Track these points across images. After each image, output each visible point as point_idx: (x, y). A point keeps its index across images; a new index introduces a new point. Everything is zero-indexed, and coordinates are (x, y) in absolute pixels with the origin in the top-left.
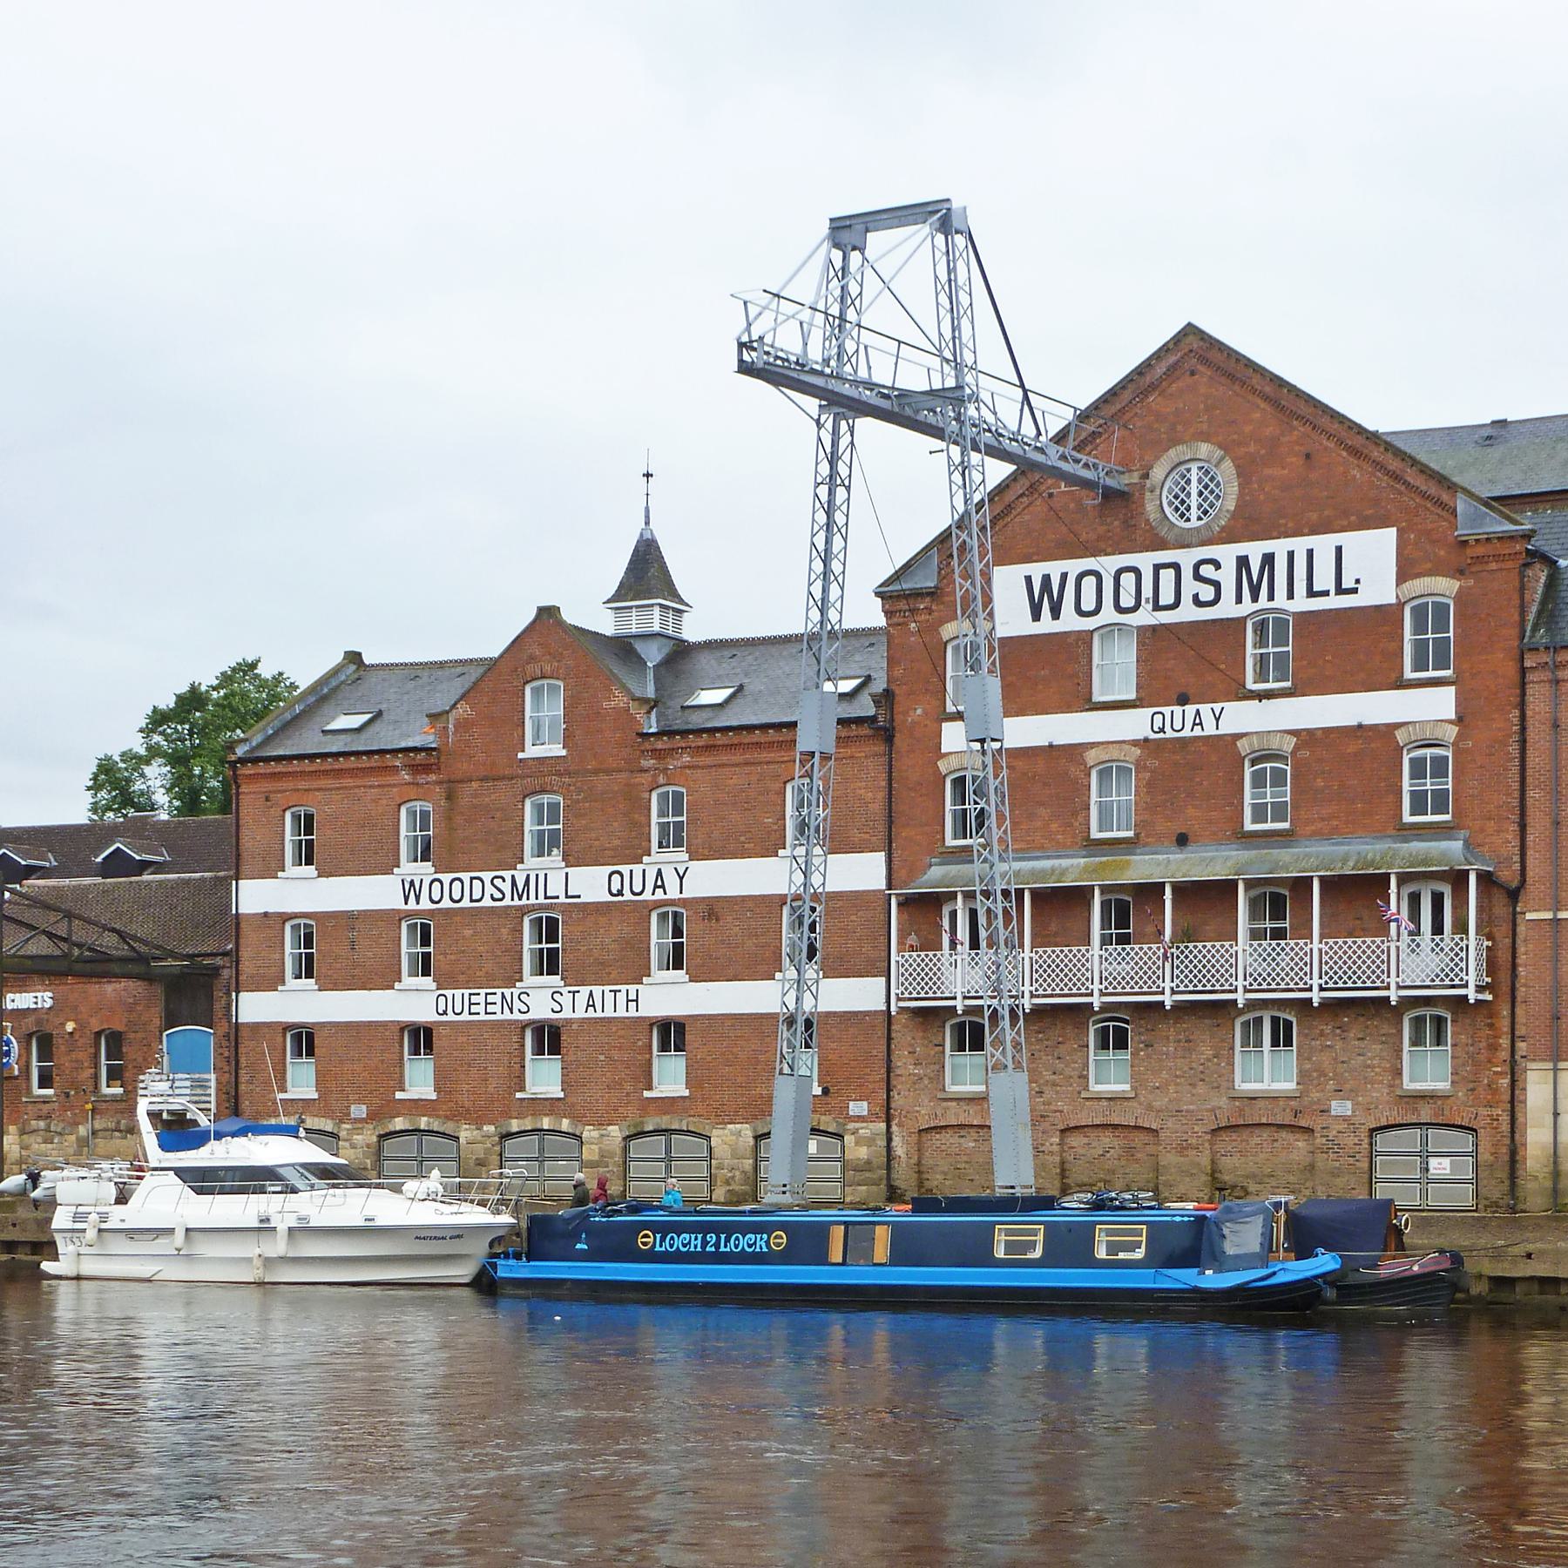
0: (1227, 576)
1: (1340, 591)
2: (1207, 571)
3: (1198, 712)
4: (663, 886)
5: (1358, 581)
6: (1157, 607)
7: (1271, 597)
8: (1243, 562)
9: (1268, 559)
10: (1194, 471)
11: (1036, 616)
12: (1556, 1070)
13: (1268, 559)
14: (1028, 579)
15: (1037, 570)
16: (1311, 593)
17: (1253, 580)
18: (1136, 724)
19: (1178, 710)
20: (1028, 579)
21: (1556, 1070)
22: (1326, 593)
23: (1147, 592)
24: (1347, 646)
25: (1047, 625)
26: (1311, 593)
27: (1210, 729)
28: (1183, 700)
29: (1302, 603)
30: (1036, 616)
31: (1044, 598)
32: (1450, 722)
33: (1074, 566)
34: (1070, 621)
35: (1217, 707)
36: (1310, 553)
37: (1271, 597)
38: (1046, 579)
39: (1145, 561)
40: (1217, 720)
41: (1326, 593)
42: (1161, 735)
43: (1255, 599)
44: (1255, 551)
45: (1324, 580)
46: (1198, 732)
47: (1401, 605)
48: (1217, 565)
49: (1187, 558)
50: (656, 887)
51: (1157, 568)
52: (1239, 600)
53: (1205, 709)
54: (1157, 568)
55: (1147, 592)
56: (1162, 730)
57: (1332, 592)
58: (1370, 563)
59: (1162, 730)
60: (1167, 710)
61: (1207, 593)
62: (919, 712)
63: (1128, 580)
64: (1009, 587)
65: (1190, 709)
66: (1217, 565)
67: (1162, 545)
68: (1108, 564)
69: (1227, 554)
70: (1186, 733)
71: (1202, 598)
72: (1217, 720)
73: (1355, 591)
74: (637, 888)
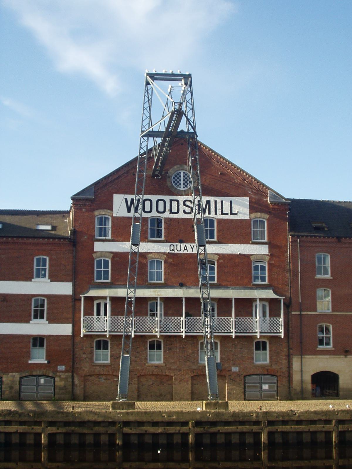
1: (232, 214)
5: (238, 212)
6: (171, 212)
7: (209, 213)
9: (208, 202)
12: (302, 358)
13: (208, 202)
14: (126, 200)
16: (222, 213)
18: (164, 248)
19: (179, 244)
20: (126, 200)
21: (302, 358)
22: (227, 214)
23: (168, 208)
24: (233, 231)
26: (222, 213)
28: (181, 242)
29: (219, 216)
30: (129, 211)
32: (267, 255)
36: (222, 202)
37: (209, 213)
39: (167, 198)
40: (192, 249)
41: (227, 214)
42: (173, 252)
45: (227, 210)
46: (186, 252)
47: (251, 219)
49: (181, 199)
51: (171, 201)
54: (171, 201)
55: (168, 208)
57: (229, 214)
58: (241, 208)
59: (173, 250)
60: (175, 244)
63: (161, 204)
67: (173, 194)
70: (182, 252)
71: (187, 211)
72: (192, 249)
73: (236, 214)
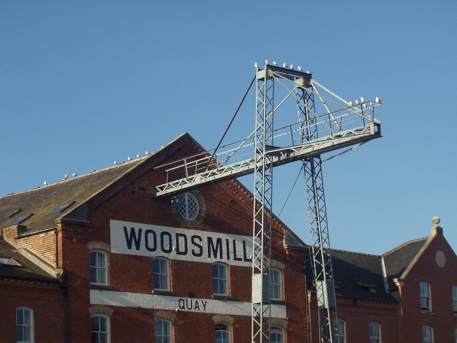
0: (204, 244)
2: (197, 240)
3: (197, 302)
4: (198, 307)
6: (179, 253)
7: (221, 257)
8: (210, 240)
9: (219, 241)
10: (186, 196)
11: (130, 247)
13: (219, 241)
14: (125, 228)
15: (129, 225)
17: (215, 248)
19: (189, 300)
20: (125, 228)
22: (240, 260)
25: (133, 251)
26: (236, 259)
27: (202, 310)
28: (192, 296)
30: (130, 247)
31: (132, 239)
33: (145, 227)
34: (143, 252)
35: (204, 300)
37: (221, 257)
38: (133, 230)
40: (205, 306)
41: (240, 260)
42: (183, 310)
43: (215, 257)
44: (215, 236)
48: (201, 240)
49: (190, 233)
50: (196, 307)
51: (178, 235)
52: (209, 256)
53: (200, 301)
54: (178, 235)
56: (183, 308)
59: (183, 308)
61: (197, 250)
62: (78, 282)
64: (117, 228)
65: (194, 300)
66: (201, 240)
68: (158, 229)
69: (205, 235)
70: (193, 310)
72: (205, 306)
74: (190, 307)
